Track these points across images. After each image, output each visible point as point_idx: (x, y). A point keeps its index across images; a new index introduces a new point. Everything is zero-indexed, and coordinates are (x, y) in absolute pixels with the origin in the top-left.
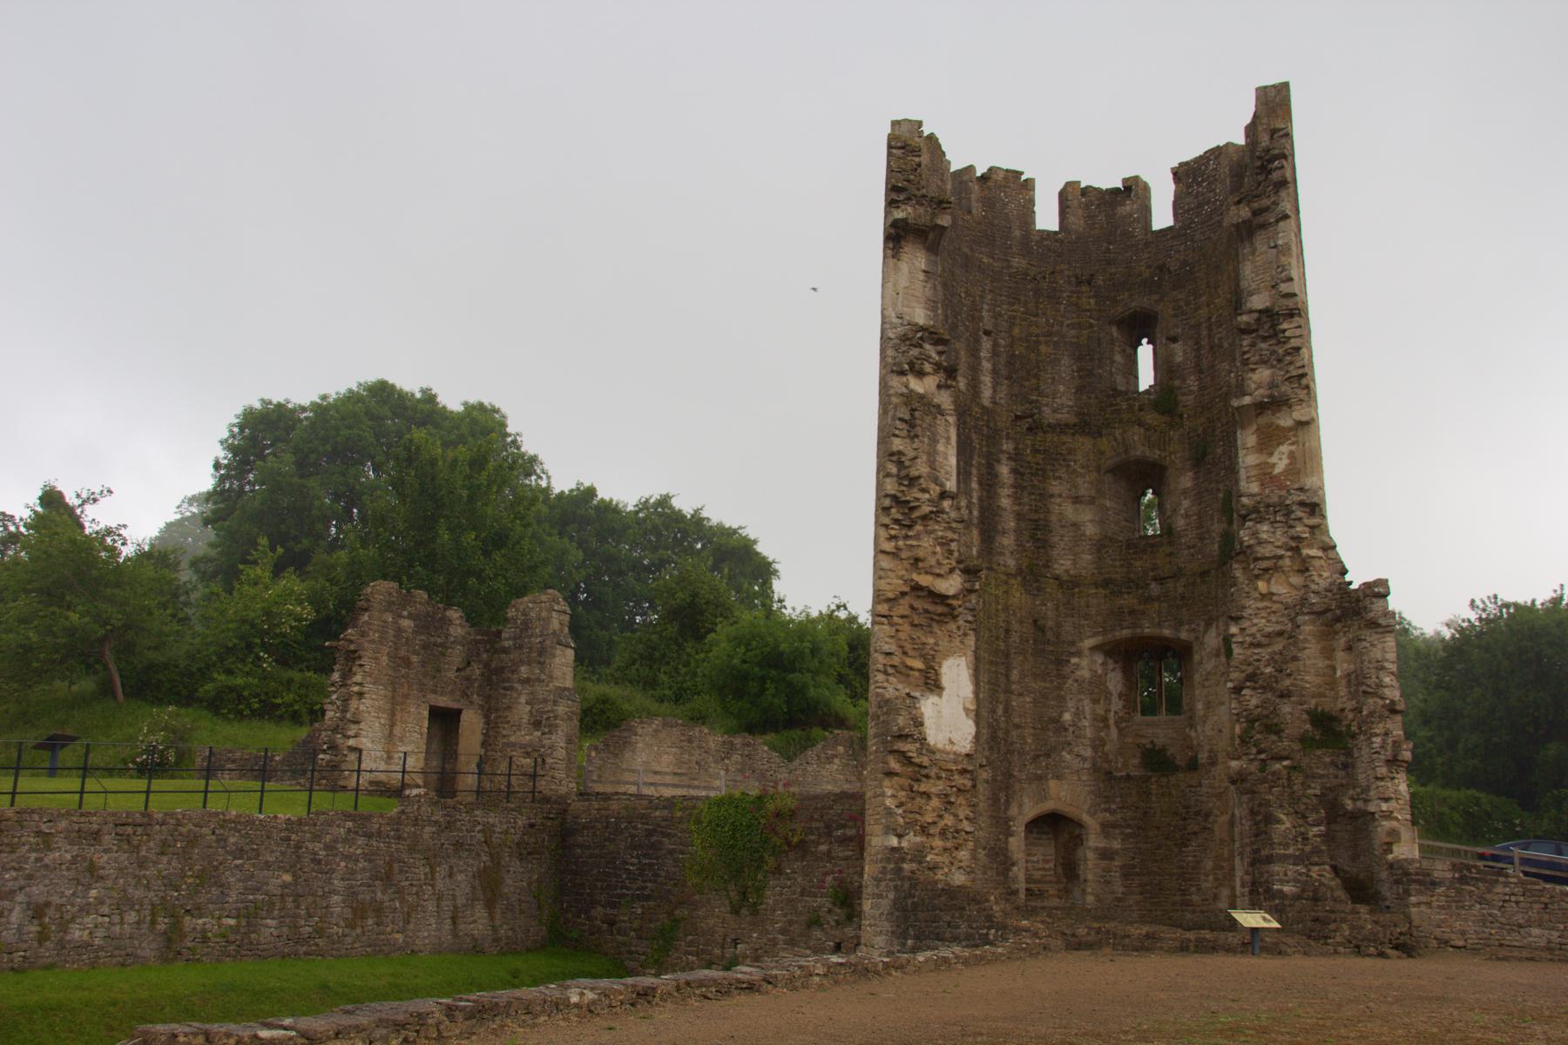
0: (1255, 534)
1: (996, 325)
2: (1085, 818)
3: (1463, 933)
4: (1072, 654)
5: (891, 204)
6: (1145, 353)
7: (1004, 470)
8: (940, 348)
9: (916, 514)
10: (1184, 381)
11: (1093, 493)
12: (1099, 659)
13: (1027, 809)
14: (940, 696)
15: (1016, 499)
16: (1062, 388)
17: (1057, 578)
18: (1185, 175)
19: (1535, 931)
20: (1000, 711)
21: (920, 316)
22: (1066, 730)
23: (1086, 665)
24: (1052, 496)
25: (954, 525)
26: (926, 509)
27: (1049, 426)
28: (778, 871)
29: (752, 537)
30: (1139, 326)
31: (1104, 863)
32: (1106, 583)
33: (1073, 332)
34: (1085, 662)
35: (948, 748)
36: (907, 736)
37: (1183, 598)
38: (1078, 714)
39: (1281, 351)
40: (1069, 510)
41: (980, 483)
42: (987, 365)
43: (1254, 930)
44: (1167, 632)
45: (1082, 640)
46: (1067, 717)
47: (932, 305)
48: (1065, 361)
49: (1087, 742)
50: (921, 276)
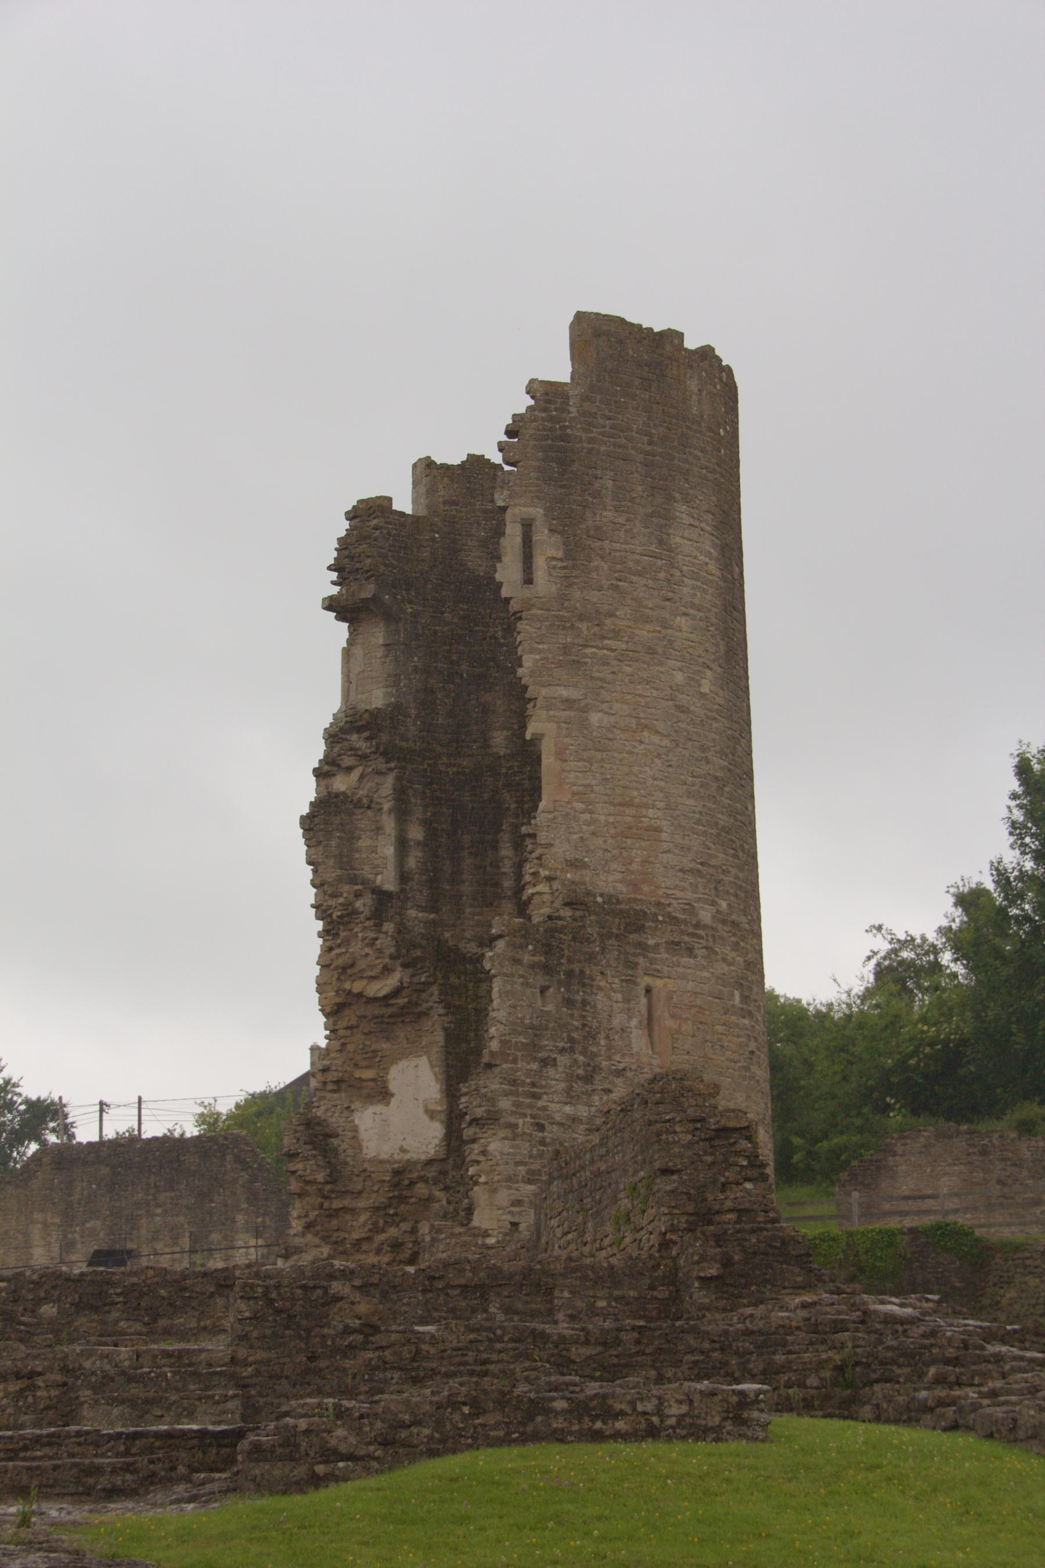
8: (366, 734)
14: (388, 1104)
21: (378, 698)
25: (368, 923)
35: (396, 1157)
36: (296, 1155)
47: (394, 680)
50: (380, 652)
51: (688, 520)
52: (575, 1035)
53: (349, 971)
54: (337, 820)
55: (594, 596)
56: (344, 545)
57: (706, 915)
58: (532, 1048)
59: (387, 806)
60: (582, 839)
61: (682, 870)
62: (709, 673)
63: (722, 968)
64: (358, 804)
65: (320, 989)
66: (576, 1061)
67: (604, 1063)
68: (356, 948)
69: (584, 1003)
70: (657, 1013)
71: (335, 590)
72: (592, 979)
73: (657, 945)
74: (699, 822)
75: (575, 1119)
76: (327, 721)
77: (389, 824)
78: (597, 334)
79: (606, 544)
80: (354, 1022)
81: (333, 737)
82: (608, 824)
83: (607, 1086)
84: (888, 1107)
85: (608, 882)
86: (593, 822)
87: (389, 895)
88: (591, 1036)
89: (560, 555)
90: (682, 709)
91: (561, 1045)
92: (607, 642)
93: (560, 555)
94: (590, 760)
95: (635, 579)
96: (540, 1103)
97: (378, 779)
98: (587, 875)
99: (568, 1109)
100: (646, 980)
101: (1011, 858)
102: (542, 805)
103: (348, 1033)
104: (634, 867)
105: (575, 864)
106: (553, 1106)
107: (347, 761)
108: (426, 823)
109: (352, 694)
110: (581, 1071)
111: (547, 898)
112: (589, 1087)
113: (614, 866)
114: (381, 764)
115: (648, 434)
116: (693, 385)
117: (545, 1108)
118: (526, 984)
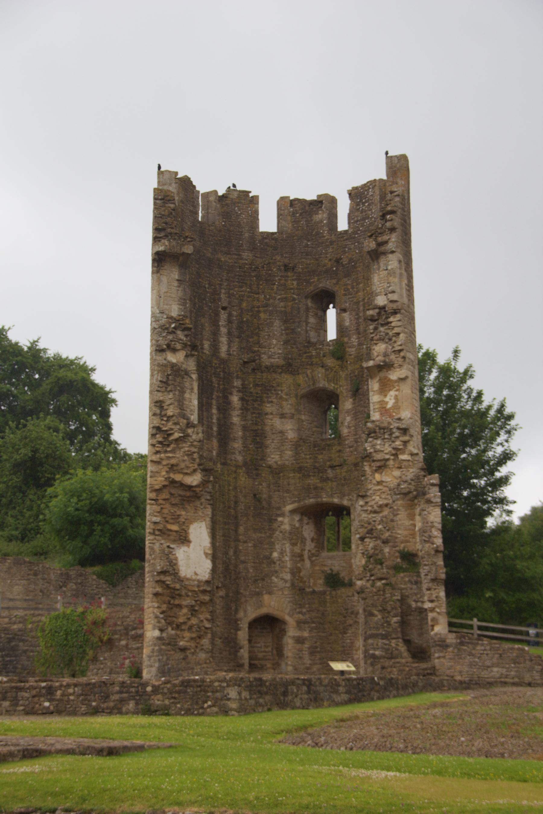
0: (373, 446)
1: (230, 303)
2: (287, 618)
3: (460, 672)
4: (279, 515)
5: (156, 239)
6: (331, 314)
7: (235, 399)
8: (186, 333)
9: (172, 438)
10: (350, 339)
11: (293, 411)
12: (297, 518)
13: (250, 612)
14: (189, 546)
15: (243, 417)
16: (274, 342)
17: (270, 467)
18: (357, 195)
19: (495, 669)
20: (231, 552)
21: (175, 311)
22: (274, 563)
23: (286, 523)
24: (267, 414)
26: (177, 435)
27: (267, 367)
28: (95, 659)
29: (90, 364)
30: (325, 299)
31: (298, 646)
32: (300, 469)
33: (282, 304)
34: (286, 520)
35: (194, 577)
37: (345, 479)
38: (282, 553)
39: (391, 334)
40: (277, 423)
41: (219, 409)
42: (224, 330)
43: (342, 673)
44: (336, 500)
45: (285, 506)
46: (275, 555)
47: (182, 302)
48: (277, 323)
49: (288, 570)
50: (176, 284)
53: (175, 468)
103: (164, 502)
109: (162, 304)
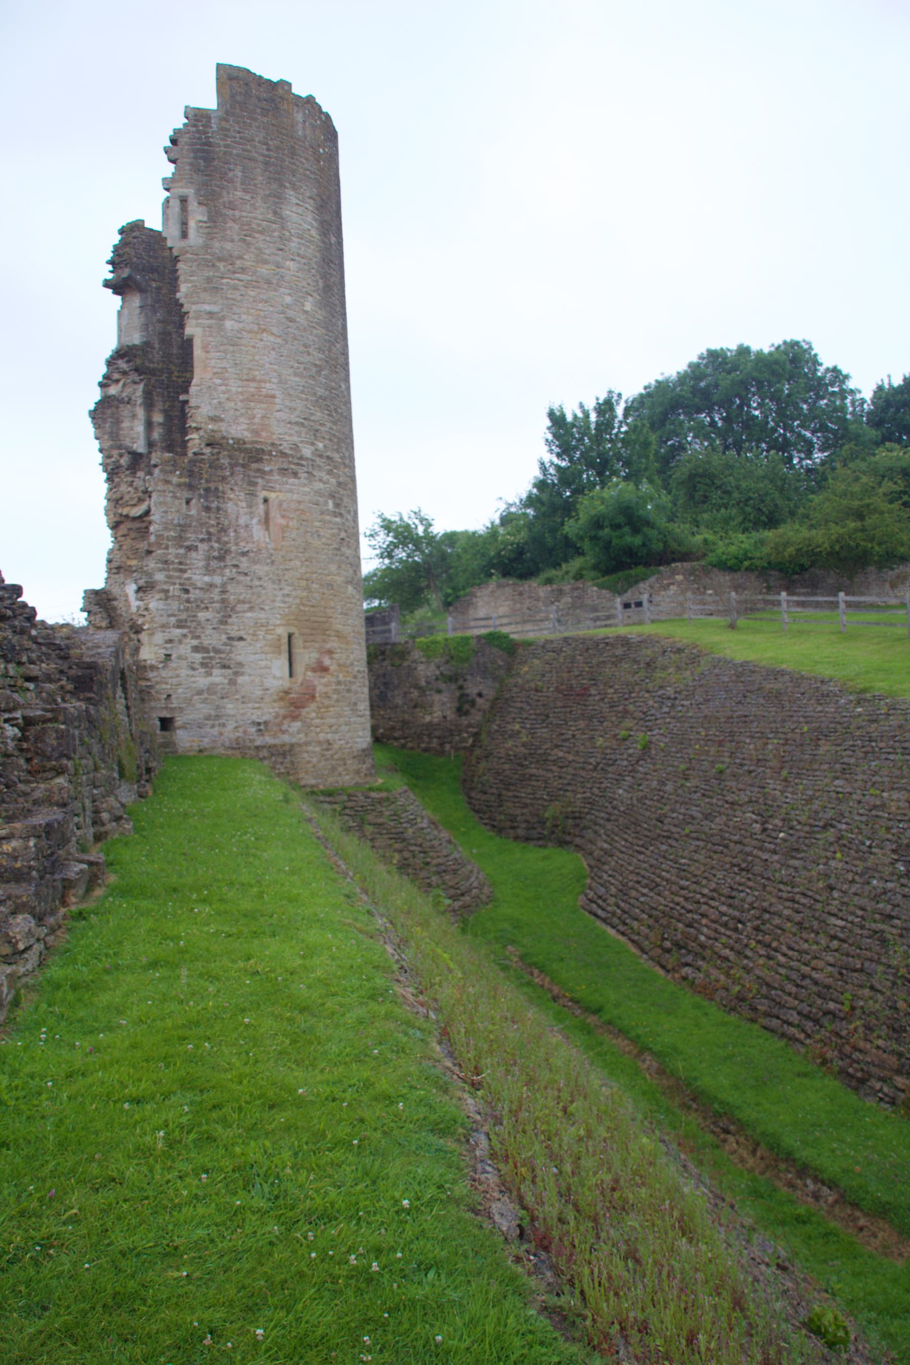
21: (136, 339)
47: (145, 327)
50: (138, 311)
51: (295, 201)
52: (212, 530)
54: (109, 411)
55: (228, 246)
56: (117, 249)
57: (307, 451)
58: (180, 538)
59: (139, 401)
60: (220, 403)
61: (290, 423)
62: (310, 298)
63: (319, 486)
64: (121, 401)
65: (107, 514)
66: (212, 547)
67: (233, 548)
68: (124, 488)
69: (218, 509)
70: (272, 514)
71: (110, 276)
72: (224, 493)
73: (271, 471)
74: (302, 392)
75: (211, 585)
76: (108, 354)
77: (140, 412)
78: (231, 79)
79: (237, 213)
80: (125, 532)
81: (110, 363)
82: (238, 393)
83: (235, 562)
84: (492, 574)
85: (238, 430)
86: (229, 391)
87: (141, 455)
88: (224, 530)
89: (205, 219)
90: (291, 320)
91: (201, 536)
92: (237, 275)
93: (205, 219)
94: (225, 352)
95: (257, 235)
96: (186, 576)
97: (136, 386)
98: (223, 426)
99: (207, 579)
100: (264, 494)
101: (549, 458)
102: (194, 382)
104: (256, 420)
105: (214, 419)
106: (195, 577)
107: (116, 376)
108: (165, 412)
110: (216, 554)
111: (197, 442)
112: (222, 564)
113: (242, 420)
114: (135, 377)
115: (266, 144)
116: (299, 117)
117: (189, 579)
118: (175, 497)
